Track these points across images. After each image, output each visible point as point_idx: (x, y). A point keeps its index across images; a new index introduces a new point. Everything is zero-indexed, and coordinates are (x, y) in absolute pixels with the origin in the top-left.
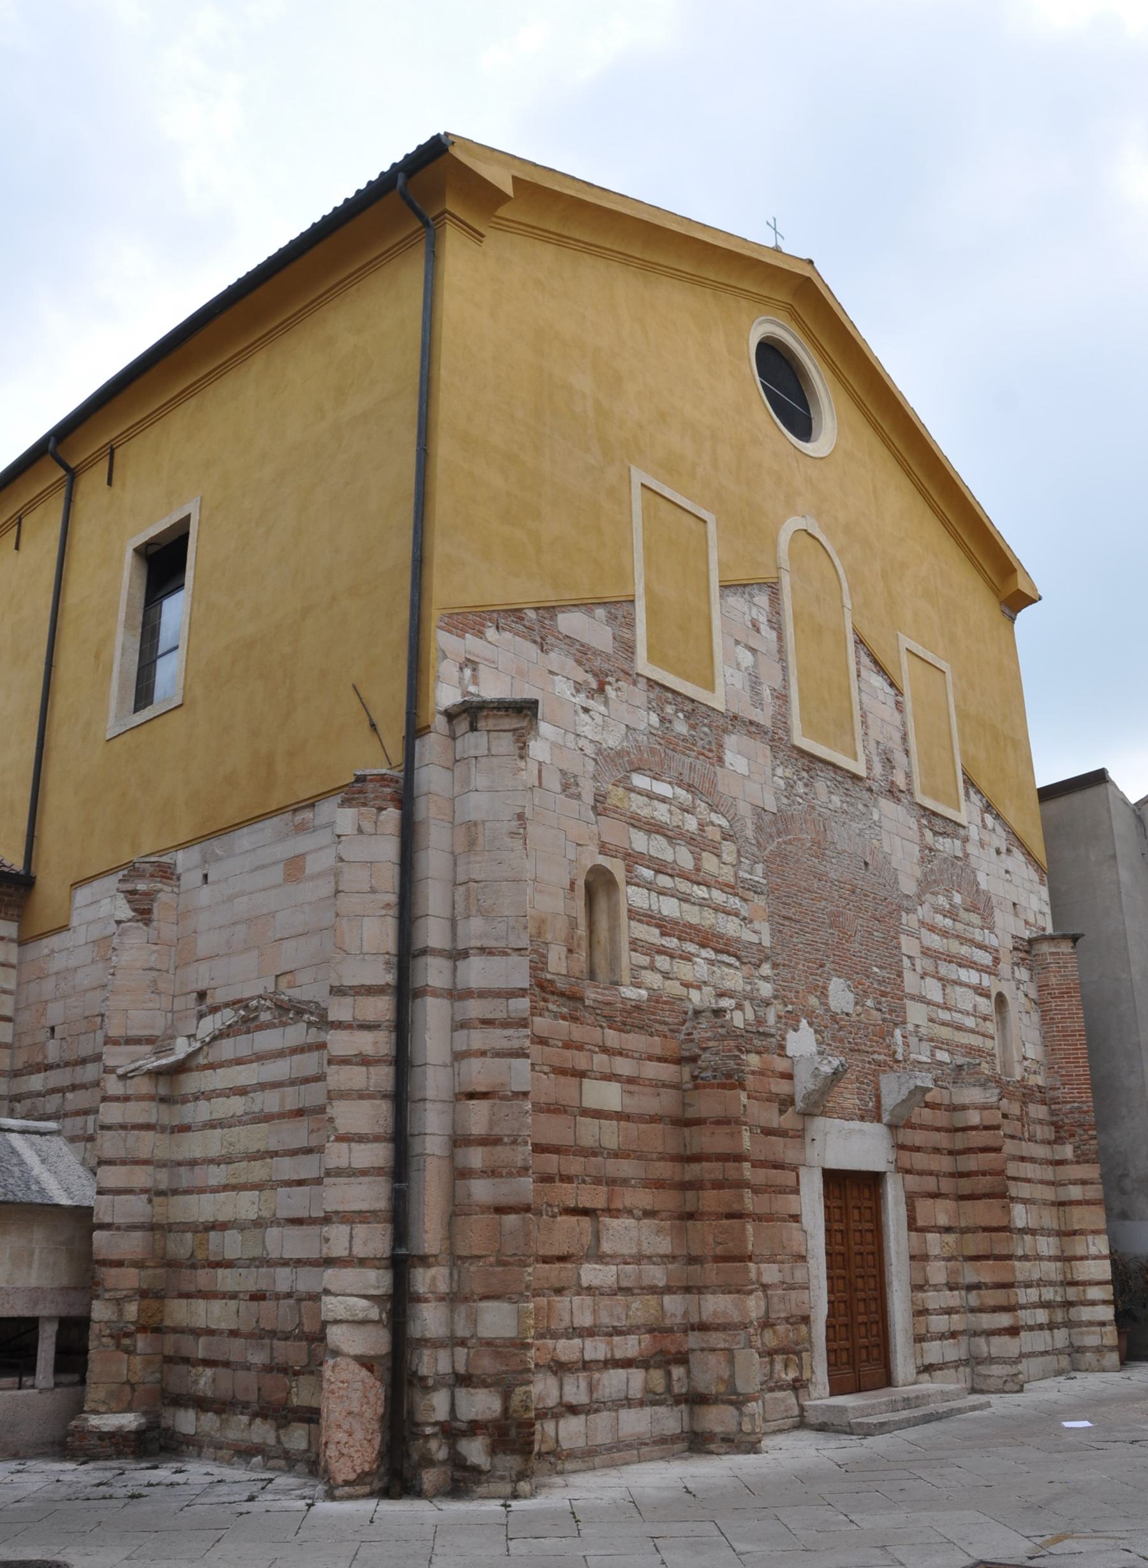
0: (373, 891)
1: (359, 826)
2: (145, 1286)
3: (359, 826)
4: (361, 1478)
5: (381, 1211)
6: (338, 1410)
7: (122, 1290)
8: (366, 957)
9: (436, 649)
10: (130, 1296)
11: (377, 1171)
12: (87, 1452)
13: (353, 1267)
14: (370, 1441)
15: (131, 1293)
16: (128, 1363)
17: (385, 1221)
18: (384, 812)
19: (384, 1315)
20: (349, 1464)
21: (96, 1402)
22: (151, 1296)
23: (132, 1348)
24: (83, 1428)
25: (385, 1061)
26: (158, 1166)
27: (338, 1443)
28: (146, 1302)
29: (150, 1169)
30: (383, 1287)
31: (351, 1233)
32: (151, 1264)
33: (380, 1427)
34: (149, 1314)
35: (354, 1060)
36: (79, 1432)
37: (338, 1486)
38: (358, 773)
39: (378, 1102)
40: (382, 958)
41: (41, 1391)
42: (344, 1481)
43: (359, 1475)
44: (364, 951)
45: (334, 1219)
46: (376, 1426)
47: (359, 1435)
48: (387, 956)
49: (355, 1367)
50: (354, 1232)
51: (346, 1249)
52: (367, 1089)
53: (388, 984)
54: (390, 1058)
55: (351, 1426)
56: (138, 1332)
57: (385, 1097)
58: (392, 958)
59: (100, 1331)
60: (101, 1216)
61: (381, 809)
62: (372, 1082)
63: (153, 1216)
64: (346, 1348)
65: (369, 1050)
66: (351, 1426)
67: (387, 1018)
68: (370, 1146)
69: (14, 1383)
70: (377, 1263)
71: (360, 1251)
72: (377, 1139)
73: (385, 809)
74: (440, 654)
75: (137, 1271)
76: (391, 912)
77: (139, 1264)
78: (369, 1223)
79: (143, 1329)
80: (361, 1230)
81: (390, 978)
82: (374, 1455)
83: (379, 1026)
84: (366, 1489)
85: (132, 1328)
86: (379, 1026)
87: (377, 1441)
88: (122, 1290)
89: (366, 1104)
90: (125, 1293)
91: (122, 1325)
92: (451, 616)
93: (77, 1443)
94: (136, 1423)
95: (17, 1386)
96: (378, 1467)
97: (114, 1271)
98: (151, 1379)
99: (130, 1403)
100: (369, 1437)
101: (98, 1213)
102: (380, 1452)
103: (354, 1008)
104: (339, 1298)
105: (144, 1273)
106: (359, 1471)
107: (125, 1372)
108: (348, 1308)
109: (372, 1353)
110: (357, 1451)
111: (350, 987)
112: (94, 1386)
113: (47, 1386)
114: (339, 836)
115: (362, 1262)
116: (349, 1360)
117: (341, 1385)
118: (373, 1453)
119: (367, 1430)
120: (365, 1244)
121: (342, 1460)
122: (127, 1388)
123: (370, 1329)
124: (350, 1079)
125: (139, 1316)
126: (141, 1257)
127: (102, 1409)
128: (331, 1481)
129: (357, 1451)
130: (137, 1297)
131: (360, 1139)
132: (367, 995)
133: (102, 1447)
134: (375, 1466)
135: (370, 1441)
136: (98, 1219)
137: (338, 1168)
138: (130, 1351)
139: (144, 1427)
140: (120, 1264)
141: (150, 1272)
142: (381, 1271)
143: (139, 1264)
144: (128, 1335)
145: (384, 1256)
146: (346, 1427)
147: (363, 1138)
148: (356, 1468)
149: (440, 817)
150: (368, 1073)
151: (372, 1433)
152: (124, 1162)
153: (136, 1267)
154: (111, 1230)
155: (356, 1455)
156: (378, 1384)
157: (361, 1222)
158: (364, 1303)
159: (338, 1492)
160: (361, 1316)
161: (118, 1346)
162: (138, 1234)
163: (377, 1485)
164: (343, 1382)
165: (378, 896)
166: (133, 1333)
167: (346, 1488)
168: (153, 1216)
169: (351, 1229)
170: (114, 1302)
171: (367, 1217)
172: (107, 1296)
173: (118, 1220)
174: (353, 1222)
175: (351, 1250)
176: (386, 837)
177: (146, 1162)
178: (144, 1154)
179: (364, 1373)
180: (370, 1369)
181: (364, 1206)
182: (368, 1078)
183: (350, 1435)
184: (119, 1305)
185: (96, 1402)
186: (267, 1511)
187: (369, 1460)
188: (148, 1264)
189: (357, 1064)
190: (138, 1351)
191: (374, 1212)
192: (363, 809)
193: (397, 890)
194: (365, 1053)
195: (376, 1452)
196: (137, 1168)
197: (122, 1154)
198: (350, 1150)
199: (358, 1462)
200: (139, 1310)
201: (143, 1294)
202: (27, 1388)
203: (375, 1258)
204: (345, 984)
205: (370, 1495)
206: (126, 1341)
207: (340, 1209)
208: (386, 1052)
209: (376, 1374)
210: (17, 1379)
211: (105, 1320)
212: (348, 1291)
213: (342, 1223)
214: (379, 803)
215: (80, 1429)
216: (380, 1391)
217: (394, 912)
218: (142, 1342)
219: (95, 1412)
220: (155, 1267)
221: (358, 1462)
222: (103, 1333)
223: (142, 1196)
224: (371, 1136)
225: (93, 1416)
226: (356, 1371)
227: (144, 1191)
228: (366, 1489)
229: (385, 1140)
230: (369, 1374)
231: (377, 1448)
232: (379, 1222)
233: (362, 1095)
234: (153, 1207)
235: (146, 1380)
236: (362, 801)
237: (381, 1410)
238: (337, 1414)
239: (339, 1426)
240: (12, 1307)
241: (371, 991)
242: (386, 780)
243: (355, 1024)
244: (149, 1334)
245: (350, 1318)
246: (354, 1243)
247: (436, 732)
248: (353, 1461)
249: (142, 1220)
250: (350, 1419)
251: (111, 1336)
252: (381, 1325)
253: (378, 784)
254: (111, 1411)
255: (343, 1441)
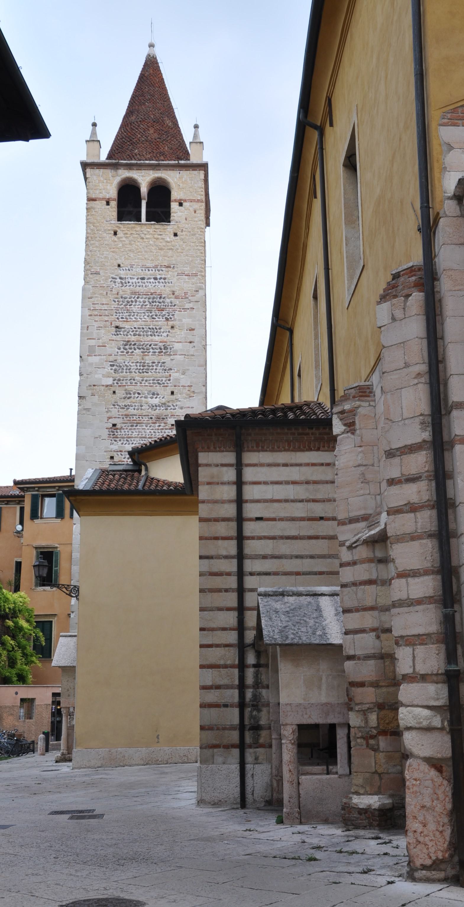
0: (407, 365)
1: (393, 315)
2: (381, 701)
3: (393, 315)
4: (436, 865)
5: (434, 633)
6: (413, 803)
7: (366, 704)
8: (406, 421)
9: (440, 145)
10: (371, 709)
11: (429, 600)
12: (353, 823)
13: (418, 682)
14: (441, 832)
15: (372, 706)
16: (375, 758)
17: (438, 642)
18: (410, 298)
19: (446, 723)
20: (425, 851)
21: (357, 786)
22: (387, 708)
23: (376, 747)
24: (349, 804)
25: (427, 506)
26: (381, 611)
27: (415, 832)
28: (383, 713)
29: (375, 613)
30: (442, 698)
31: (413, 654)
32: (383, 684)
33: (450, 821)
34: (387, 721)
35: (405, 508)
36: (348, 807)
37: (417, 870)
38: (394, 272)
39: (424, 541)
40: (418, 420)
41: (340, 776)
42: (422, 865)
43: (434, 862)
44: (404, 417)
45: (400, 643)
46: (446, 820)
47: (432, 826)
48: (421, 418)
49: (425, 767)
50: (415, 653)
51: (411, 667)
52: (416, 531)
53: (424, 441)
54: (432, 503)
55: (425, 818)
56: (379, 735)
57: (430, 536)
58: (426, 418)
59: (355, 734)
60: (347, 650)
61: (408, 296)
62: (419, 524)
63: (382, 648)
64: (415, 751)
65: (415, 499)
66: (425, 818)
67: (426, 469)
68: (422, 579)
69: (323, 770)
70: (435, 678)
71: (421, 669)
72: (426, 572)
73: (411, 295)
74: (445, 148)
75: (374, 689)
76: (423, 380)
77: (375, 685)
78: (426, 644)
79: (384, 733)
80: (420, 650)
81: (427, 435)
82: (445, 845)
83: (420, 477)
84: (442, 875)
85: (375, 732)
86: (420, 477)
87: (448, 832)
88: (366, 704)
89: (416, 544)
90: (368, 706)
91: (368, 729)
92: (454, 110)
93: (347, 815)
94: (378, 803)
95: (325, 772)
96: (451, 856)
97: (360, 690)
98: (394, 770)
99: (379, 787)
100: (441, 829)
101: (345, 649)
102: (450, 843)
103: (401, 466)
104: (409, 708)
105: (379, 691)
106: (434, 858)
107: (374, 764)
108: (415, 717)
109: (439, 756)
110: (431, 840)
111: (397, 449)
112: (355, 774)
113: (344, 773)
114: (380, 328)
115: (424, 678)
116: (419, 761)
117: (414, 782)
118: (444, 843)
119: (438, 822)
120: (424, 662)
121: (419, 847)
122: (377, 777)
123: (436, 735)
124: (403, 525)
125: (378, 723)
126: (375, 679)
127: (362, 791)
128: (411, 864)
129: (431, 840)
130: (376, 709)
131: (414, 574)
132: (410, 453)
133: (361, 820)
134: (447, 855)
135: (441, 832)
136: (346, 652)
137: (400, 600)
138: (376, 749)
139: (388, 807)
140: (362, 684)
141: (384, 690)
142: (440, 686)
143: (375, 685)
144: (373, 737)
145: (440, 672)
146: (421, 818)
147: (416, 573)
148: (432, 855)
149: (457, 288)
150: (416, 518)
151: (443, 826)
152: (357, 610)
153: (373, 687)
154: (355, 660)
155: (430, 844)
156: (445, 782)
157: (421, 644)
158: (426, 712)
159: (417, 875)
160: (425, 724)
161: (368, 744)
162: (372, 662)
163: (451, 872)
164: (416, 780)
165: (411, 369)
166: (376, 736)
167: (424, 872)
168: (382, 648)
169: (414, 650)
170: (362, 713)
171: (423, 640)
172: (357, 708)
173: (359, 653)
174: (415, 645)
175: (414, 669)
176: (413, 318)
177: (372, 608)
178: (369, 602)
179: (433, 773)
180: (439, 770)
181: (421, 630)
182: (416, 522)
183: (425, 826)
184: (365, 715)
185: (357, 786)
186: (352, 884)
187: (442, 849)
188: (381, 684)
189: (407, 512)
190: (381, 749)
191: (428, 635)
192: (395, 301)
193: (427, 360)
194: (412, 502)
195: (447, 843)
196: (366, 613)
197: (355, 604)
198: (407, 583)
199: (432, 850)
200: (378, 719)
201: (381, 707)
202: (334, 774)
203: (432, 675)
204: (393, 448)
205: (445, 880)
206: (372, 742)
207: (404, 633)
208: (427, 498)
209: (444, 774)
210: (325, 767)
211: (357, 726)
212: (415, 703)
213: (406, 645)
214: (406, 292)
215: (347, 805)
216: (447, 789)
217: (425, 379)
218: (383, 742)
219: (357, 793)
220: (388, 686)
221: (432, 850)
222: (357, 736)
223: (371, 634)
224: (422, 571)
225: (355, 796)
226: (426, 770)
227: (373, 630)
228: (442, 875)
229: (433, 573)
230: (437, 773)
231: (448, 839)
232: (433, 644)
233: (413, 537)
234: (381, 641)
235: (390, 771)
236: (394, 293)
237: (449, 806)
238: (412, 807)
239: (415, 817)
240: (310, 717)
241: (411, 449)
242: (415, 271)
243: (403, 479)
244: (389, 737)
245: (417, 726)
246: (416, 662)
247: (446, 216)
248: (428, 849)
249: (373, 652)
250: (424, 812)
251: (362, 737)
252: (445, 732)
253: (407, 276)
254: (366, 793)
255: (419, 830)
